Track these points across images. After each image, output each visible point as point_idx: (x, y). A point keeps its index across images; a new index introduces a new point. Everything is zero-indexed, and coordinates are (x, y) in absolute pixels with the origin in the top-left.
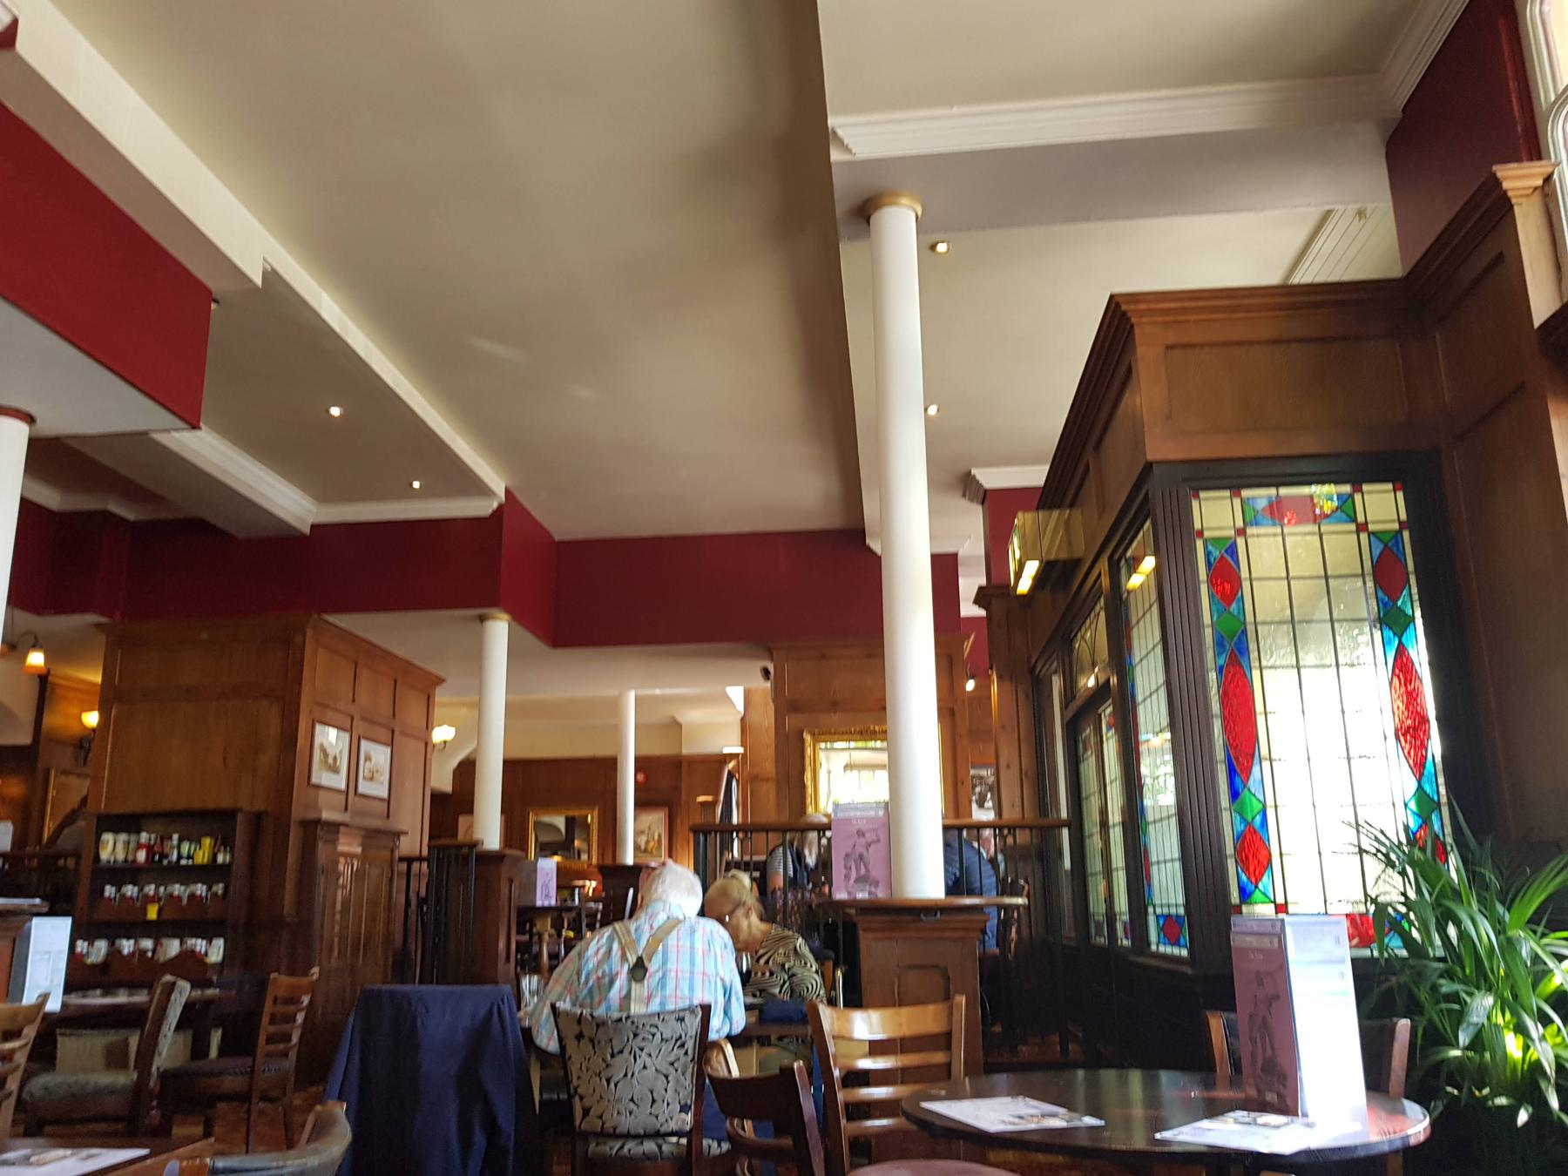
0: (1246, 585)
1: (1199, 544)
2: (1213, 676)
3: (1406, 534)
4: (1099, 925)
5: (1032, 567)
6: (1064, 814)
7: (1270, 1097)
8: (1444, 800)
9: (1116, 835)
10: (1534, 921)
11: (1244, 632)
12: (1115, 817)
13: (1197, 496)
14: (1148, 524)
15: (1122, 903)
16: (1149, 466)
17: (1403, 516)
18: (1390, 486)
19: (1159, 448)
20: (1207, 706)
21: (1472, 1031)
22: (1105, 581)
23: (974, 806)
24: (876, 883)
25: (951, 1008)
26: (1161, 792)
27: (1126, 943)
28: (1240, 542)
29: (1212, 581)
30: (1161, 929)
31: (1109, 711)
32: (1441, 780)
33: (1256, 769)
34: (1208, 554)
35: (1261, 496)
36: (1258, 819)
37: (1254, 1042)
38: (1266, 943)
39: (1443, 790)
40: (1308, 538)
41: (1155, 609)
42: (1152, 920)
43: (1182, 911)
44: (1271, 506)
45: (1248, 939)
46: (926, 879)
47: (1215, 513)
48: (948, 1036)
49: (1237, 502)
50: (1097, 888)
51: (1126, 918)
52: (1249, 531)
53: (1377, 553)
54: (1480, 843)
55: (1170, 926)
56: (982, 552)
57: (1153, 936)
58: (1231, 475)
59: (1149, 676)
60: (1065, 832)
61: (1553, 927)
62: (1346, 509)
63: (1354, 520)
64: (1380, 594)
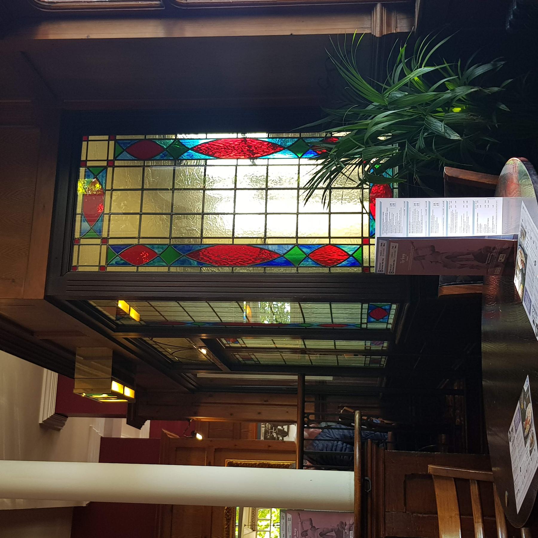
0: (142, 241)
1: (109, 269)
2: (204, 270)
3: (118, 137)
4: (372, 361)
5: (116, 387)
6: (296, 377)
7: (502, 258)
8: (298, 135)
9: (311, 344)
10: (379, 89)
11: (175, 246)
12: (298, 344)
13: (76, 267)
14: (92, 302)
15: (359, 345)
16: (46, 297)
17: (106, 137)
18: (84, 144)
19: (36, 289)
20: (225, 275)
21: (449, 131)
22: (132, 335)
23: (286, 439)
24: (343, 524)
25: (439, 477)
26: (285, 311)
27: (385, 344)
28: (111, 242)
29: (139, 263)
30: (377, 321)
31: (224, 342)
32: (285, 135)
33: (270, 248)
34: (118, 264)
35: (80, 225)
36: (305, 250)
37: (463, 266)
38: (394, 251)
39: (290, 135)
40: (114, 198)
41: (153, 303)
42: (370, 326)
43: (366, 306)
44: (88, 221)
45: (391, 262)
46: (339, 484)
47: (89, 257)
48: (456, 480)
49: (82, 241)
50: (346, 360)
51: (368, 343)
52: (105, 235)
53: (129, 156)
54: (327, 115)
55: (376, 314)
56: (103, 420)
57: (383, 326)
58: (63, 242)
59: (202, 312)
60: (307, 378)
61: (384, 79)
62: (97, 173)
63: (105, 168)
64: (158, 157)
